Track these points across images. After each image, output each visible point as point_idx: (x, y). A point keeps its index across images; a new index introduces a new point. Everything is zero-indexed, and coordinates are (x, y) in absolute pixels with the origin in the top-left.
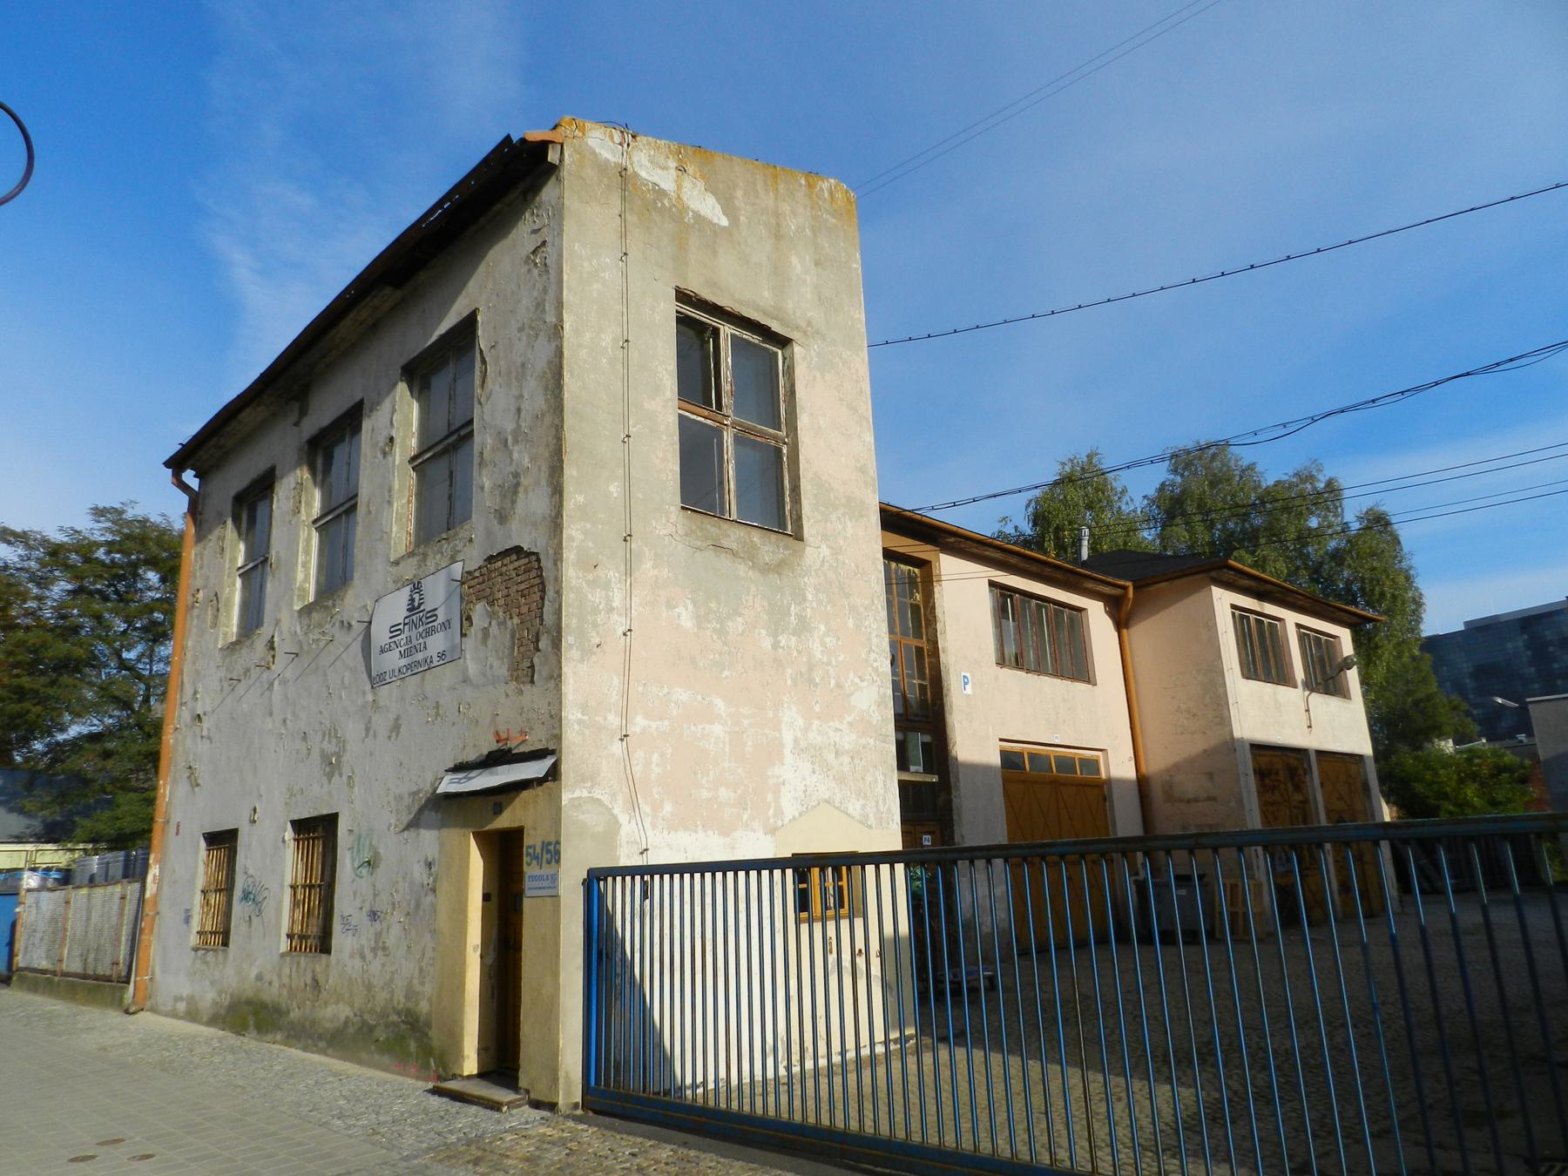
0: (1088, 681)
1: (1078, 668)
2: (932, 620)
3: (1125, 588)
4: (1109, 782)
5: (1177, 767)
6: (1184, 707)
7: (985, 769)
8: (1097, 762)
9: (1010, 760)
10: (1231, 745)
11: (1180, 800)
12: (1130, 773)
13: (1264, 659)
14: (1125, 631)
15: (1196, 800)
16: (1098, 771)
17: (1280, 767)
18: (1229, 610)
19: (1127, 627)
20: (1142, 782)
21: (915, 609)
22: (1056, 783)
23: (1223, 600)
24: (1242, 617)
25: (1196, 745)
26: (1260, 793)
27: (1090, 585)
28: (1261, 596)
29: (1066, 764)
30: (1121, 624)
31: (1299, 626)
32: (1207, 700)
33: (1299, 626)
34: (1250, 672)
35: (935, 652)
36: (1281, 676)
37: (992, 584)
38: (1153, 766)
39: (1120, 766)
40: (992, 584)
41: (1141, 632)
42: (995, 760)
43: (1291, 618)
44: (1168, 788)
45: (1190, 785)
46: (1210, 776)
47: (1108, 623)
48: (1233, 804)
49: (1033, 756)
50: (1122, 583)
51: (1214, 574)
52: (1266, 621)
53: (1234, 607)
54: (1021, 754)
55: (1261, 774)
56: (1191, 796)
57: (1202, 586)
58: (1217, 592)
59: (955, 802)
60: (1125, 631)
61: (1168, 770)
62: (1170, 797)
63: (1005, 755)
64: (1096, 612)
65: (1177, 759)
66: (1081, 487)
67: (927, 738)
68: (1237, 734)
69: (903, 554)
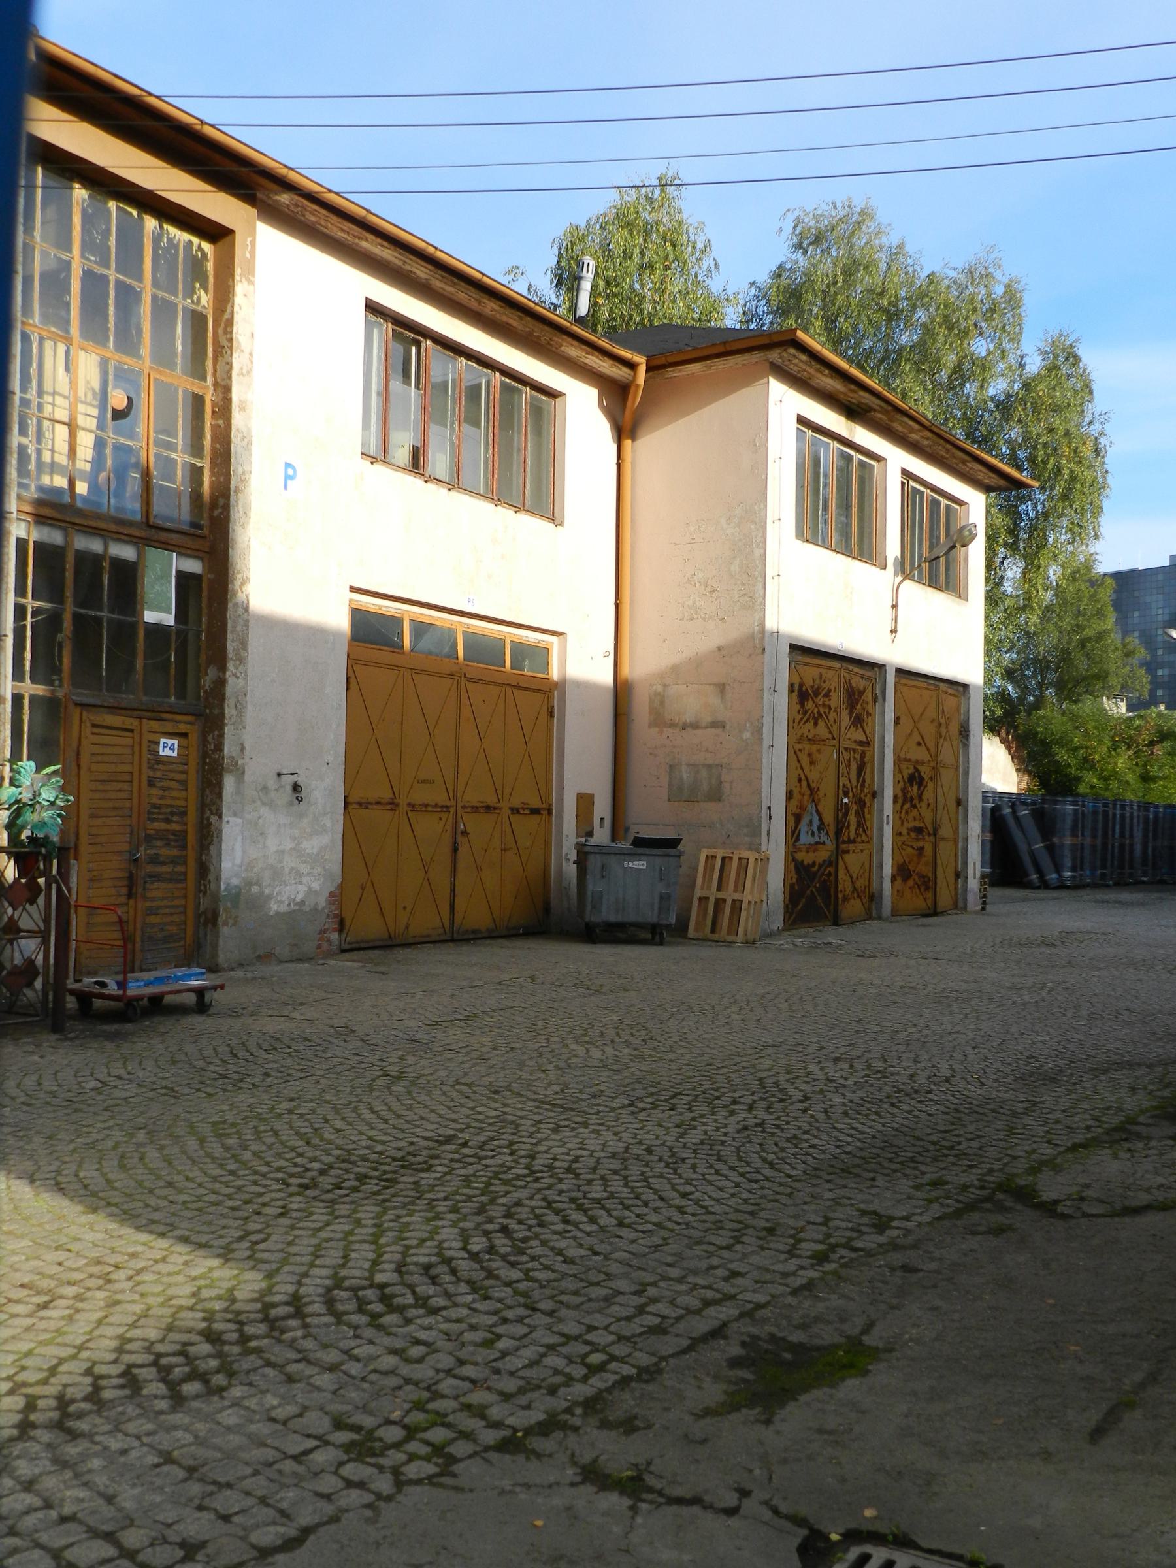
0: (552, 519)
1: (523, 478)
2: (224, 349)
3: (632, 366)
4: (561, 686)
5: (675, 669)
6: (700, 576)
7: (314, 634)
8: (546, 651)
9: (372, 633)
10: (758, 642)
11: (673, 725)
12: (606, 677)
13: (838, 512)
14: (628, 443)
15: (695, 726)
16: (546, 665)
17: (831, 686)
18: (794, 424)
19: (633, 437)
20: (622, 692)
21: (197, 320)
22: (459, 677)
23: (785, 404)
24: (815, 443)
25: (705, 638)
26: (791, 722)
27: (573, 351)
28: (853, 413)
29: (484, 650)
30: (624, 431)
31: (906, 473)
32: (735, 568)
33: (906, 473)
34: (810, 529)
35: (224, 409)
36: (860, 543)
37: (373, 308)
38: (645, 665)
39: (585, 660)
40: (373, 308)
41: (659, 444)
42: (342, 622)
43: (897, 459)
44: (659, 703)
45: (691, 702)
46: (722, 688)
47: (603, 428)
48: (747, 735)
49: (420, 629)
50: (626, 354)
51: (774, 355)
52: (857, 456)
53: (802, 420)
54: (396, 621)
55: (801, 694)
56: (688, 718)
57: (749, 378)
58: (777, 388)
59: (233, 685)
60: (628, 443)
61: (661, 675)
62: (659, 720)
63: (359, 617)
64: (581, 408)
65: (676, 658)
66: (644, 232)
67: (193, 566)
68: (771, 624)
69: (151, 194)
